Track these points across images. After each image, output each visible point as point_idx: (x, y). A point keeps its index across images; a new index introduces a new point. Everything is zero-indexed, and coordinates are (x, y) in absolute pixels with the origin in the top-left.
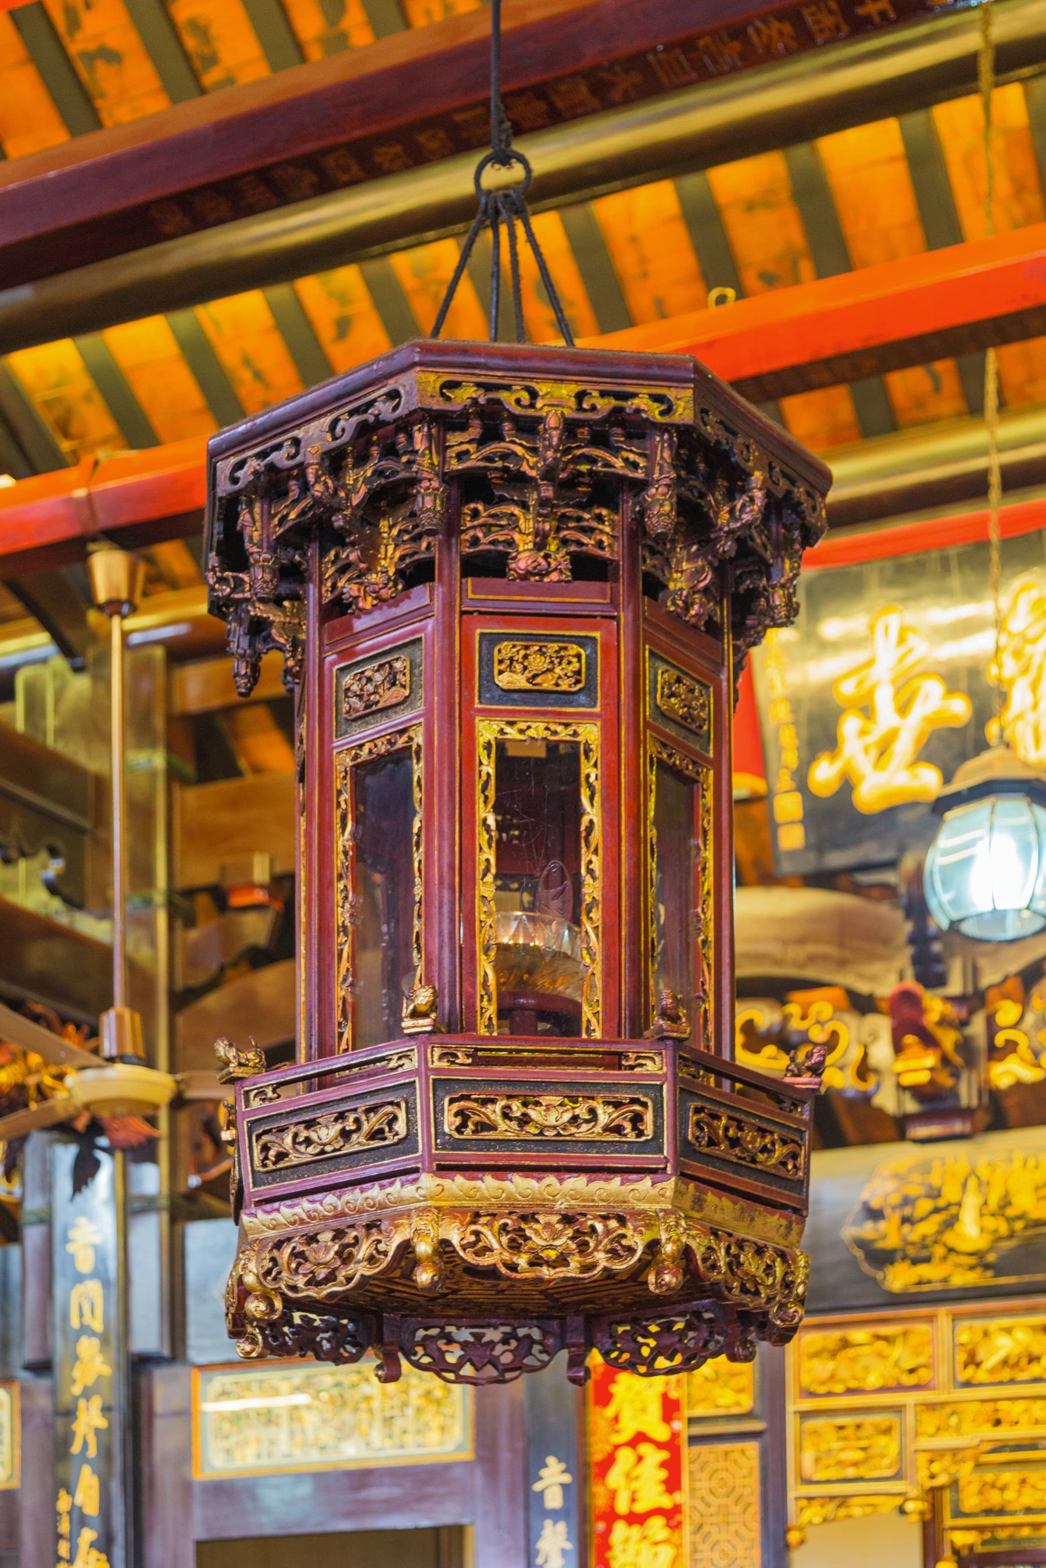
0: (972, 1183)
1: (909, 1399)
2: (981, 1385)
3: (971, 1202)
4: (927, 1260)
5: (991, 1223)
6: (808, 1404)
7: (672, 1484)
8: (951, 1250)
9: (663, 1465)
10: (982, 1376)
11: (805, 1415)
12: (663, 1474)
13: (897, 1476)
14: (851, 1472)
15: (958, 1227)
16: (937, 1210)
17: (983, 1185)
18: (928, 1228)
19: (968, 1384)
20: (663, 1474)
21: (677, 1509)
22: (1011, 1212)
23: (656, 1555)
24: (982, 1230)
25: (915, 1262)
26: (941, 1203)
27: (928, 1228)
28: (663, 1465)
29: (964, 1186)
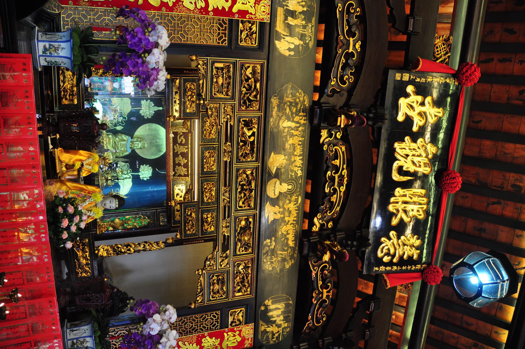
0: (298, 125)
1: (236, 102)
2: (238, 126)
3: (293, 125)
4: (279, 110)
5: (286, 130)
6: (238, 66)
7: (216, 11)
8: (280, 119)
9: (223, 8)
10: (241, 126)
11: (235, 64)
12: (220, 8)
13: (212, 97)
14: (215, 80)
15: (286, 121)
16: (292, 113)
17: (296, 128)
18: (288, 110)
19: (239, 121)
20: (220, 8)
21: (207, 13)
22: (288, 137)
23: (191, 3)
24: (285, 127)
25: (278, 106)
26: (294, 115)
27: (288, 110)
28: (223, 8)
29: (297, 122)
